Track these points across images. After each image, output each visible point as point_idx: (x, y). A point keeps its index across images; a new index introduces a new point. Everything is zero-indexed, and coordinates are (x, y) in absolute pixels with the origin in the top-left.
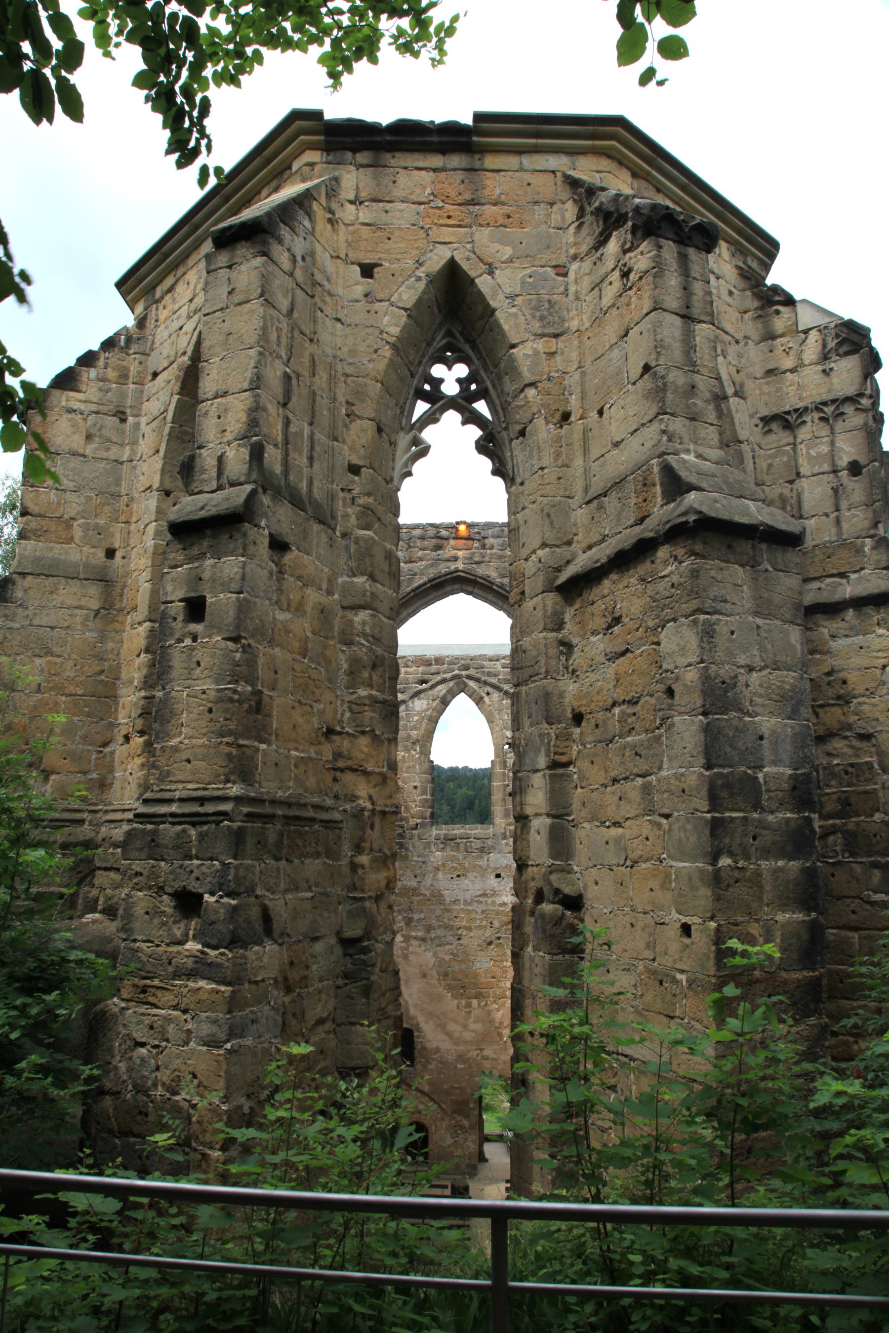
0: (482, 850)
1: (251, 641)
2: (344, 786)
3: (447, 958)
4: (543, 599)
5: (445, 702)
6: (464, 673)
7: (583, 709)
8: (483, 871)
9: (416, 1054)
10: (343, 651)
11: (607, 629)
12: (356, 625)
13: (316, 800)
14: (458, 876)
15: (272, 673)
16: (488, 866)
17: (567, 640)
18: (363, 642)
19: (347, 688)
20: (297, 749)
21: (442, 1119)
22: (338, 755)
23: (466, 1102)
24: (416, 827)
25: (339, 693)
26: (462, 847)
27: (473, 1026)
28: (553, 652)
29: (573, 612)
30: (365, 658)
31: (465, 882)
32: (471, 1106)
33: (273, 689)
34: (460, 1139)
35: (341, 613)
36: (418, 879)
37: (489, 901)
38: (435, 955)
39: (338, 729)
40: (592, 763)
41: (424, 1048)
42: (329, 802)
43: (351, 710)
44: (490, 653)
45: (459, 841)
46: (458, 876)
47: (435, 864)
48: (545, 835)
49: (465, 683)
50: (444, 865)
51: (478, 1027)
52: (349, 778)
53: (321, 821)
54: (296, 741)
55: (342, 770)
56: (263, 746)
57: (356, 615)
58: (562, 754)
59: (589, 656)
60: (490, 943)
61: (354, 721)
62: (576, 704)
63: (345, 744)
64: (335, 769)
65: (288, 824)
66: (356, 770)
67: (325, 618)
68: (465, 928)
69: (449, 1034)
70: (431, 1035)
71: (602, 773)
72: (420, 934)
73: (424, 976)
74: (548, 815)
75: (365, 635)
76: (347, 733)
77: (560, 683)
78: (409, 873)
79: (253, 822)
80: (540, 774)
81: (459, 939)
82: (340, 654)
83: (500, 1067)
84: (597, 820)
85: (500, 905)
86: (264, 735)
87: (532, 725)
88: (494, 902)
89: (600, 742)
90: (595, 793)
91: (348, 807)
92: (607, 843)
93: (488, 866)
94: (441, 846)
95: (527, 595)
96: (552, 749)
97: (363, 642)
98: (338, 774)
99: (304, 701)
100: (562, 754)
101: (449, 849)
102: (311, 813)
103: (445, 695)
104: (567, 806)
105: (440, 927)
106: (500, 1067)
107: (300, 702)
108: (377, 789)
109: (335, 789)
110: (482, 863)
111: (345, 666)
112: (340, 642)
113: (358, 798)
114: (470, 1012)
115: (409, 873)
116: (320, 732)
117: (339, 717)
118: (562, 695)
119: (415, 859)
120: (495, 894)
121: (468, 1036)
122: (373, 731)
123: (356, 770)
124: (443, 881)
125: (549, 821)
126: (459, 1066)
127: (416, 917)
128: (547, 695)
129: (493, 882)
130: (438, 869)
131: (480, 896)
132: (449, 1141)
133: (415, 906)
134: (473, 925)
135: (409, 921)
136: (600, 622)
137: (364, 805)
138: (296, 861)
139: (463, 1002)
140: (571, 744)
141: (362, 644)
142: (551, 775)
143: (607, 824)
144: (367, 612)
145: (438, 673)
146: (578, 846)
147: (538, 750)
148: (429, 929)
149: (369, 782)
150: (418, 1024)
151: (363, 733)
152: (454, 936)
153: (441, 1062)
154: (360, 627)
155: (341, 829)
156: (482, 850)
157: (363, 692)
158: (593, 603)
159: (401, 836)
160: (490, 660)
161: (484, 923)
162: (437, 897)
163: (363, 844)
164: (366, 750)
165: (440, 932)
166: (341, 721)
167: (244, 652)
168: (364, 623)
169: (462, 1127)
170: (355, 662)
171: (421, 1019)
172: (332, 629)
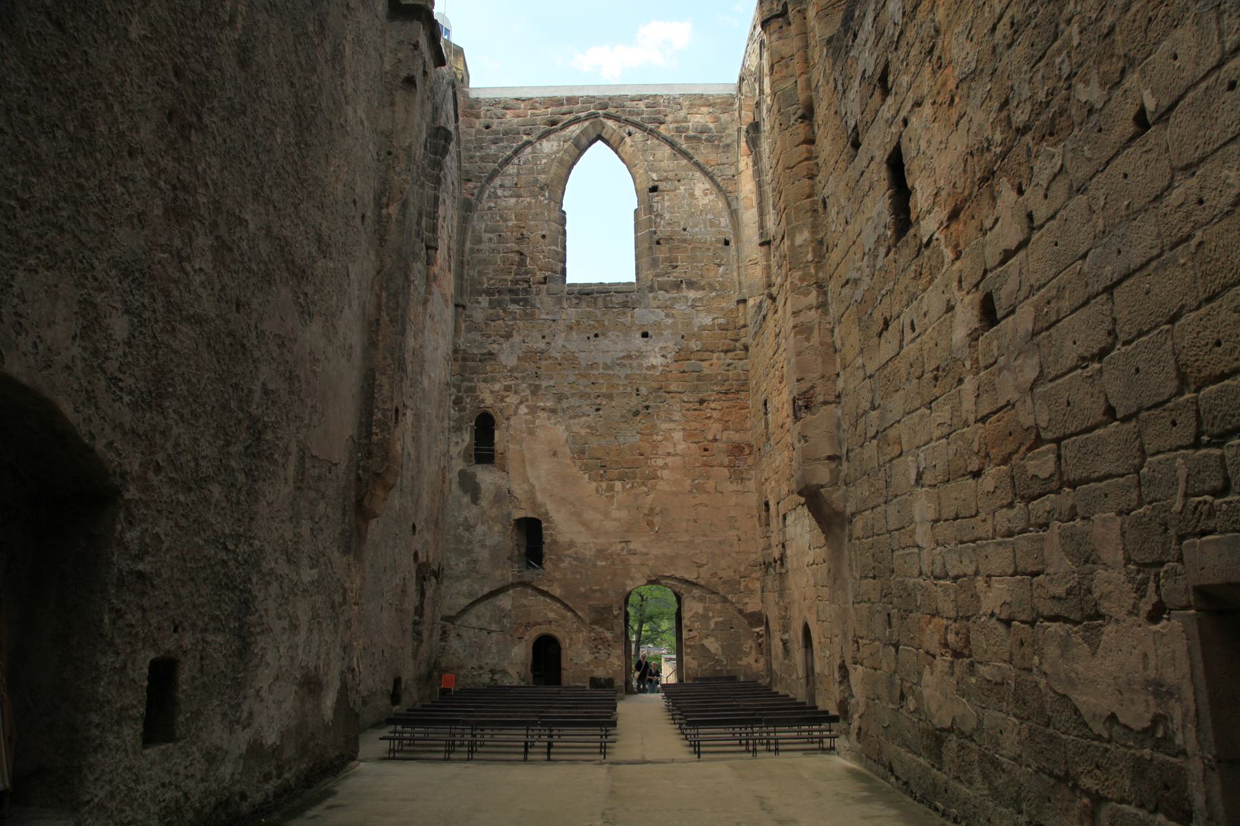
0: (625, 305)
3: (583, 432)
5: (580, 148)
6: (601, 112)
8: (627, 330)
9: (545, 549)
14: (596, 336)
16: (633, 324)
21: (579, 630)
23: (608, 609)
24: (545, 281)
26: (600, 302)
27: (616, 514)
31: (603, 343)
32: (616, 613)
34: (602, 655)
36: (547, 340)
37: (635, 364)
38: (568, 428)
41: (555, 542)
44: (632, 93)
45: (596, 295)
46: (596, 336)
47: (568, 322)
49: (602, 123)
50: (578, 323)
51: (623, 514)
60: (636, 413)
68: (605, 396)
69: (585, 524)
70: (563, 527)
72: (548, 404)
73: (555, 454)
78: (536, 333)
81: (598, 410)
83: (651, 563)
85: (648, 368)
88: (640, 365)
93: (633, 324)
94: (575, 301)
101: (584, 304)
103: (578, 136)
105: (573, 395)
106: (651, 563)
110: (627, 320)
114: (612, 497)
115: (536, 333)
119: (543, 316)
120: (641, 355)
121: (609, 525)
124: (575, 343)
126: (599, 563)
127: (544, 384)
129: (638, 341)
130: (571, 328)
131: (623, 358)
132: (588, 657)
133: (542, 372)
134: (615, 391)
135: (535, 390)
139: (604, 485)
145: (570, 113)
148: (560, 397)
150: (547, 513)
152: (591, 405)
153: (576, 559)
156: (625, 305)
159: (526, 291)
160: (633, 101)
161: (629, 390)
162: (571, 360)
165: (574, 401)
169: (603, 640)
171: (550, 507)
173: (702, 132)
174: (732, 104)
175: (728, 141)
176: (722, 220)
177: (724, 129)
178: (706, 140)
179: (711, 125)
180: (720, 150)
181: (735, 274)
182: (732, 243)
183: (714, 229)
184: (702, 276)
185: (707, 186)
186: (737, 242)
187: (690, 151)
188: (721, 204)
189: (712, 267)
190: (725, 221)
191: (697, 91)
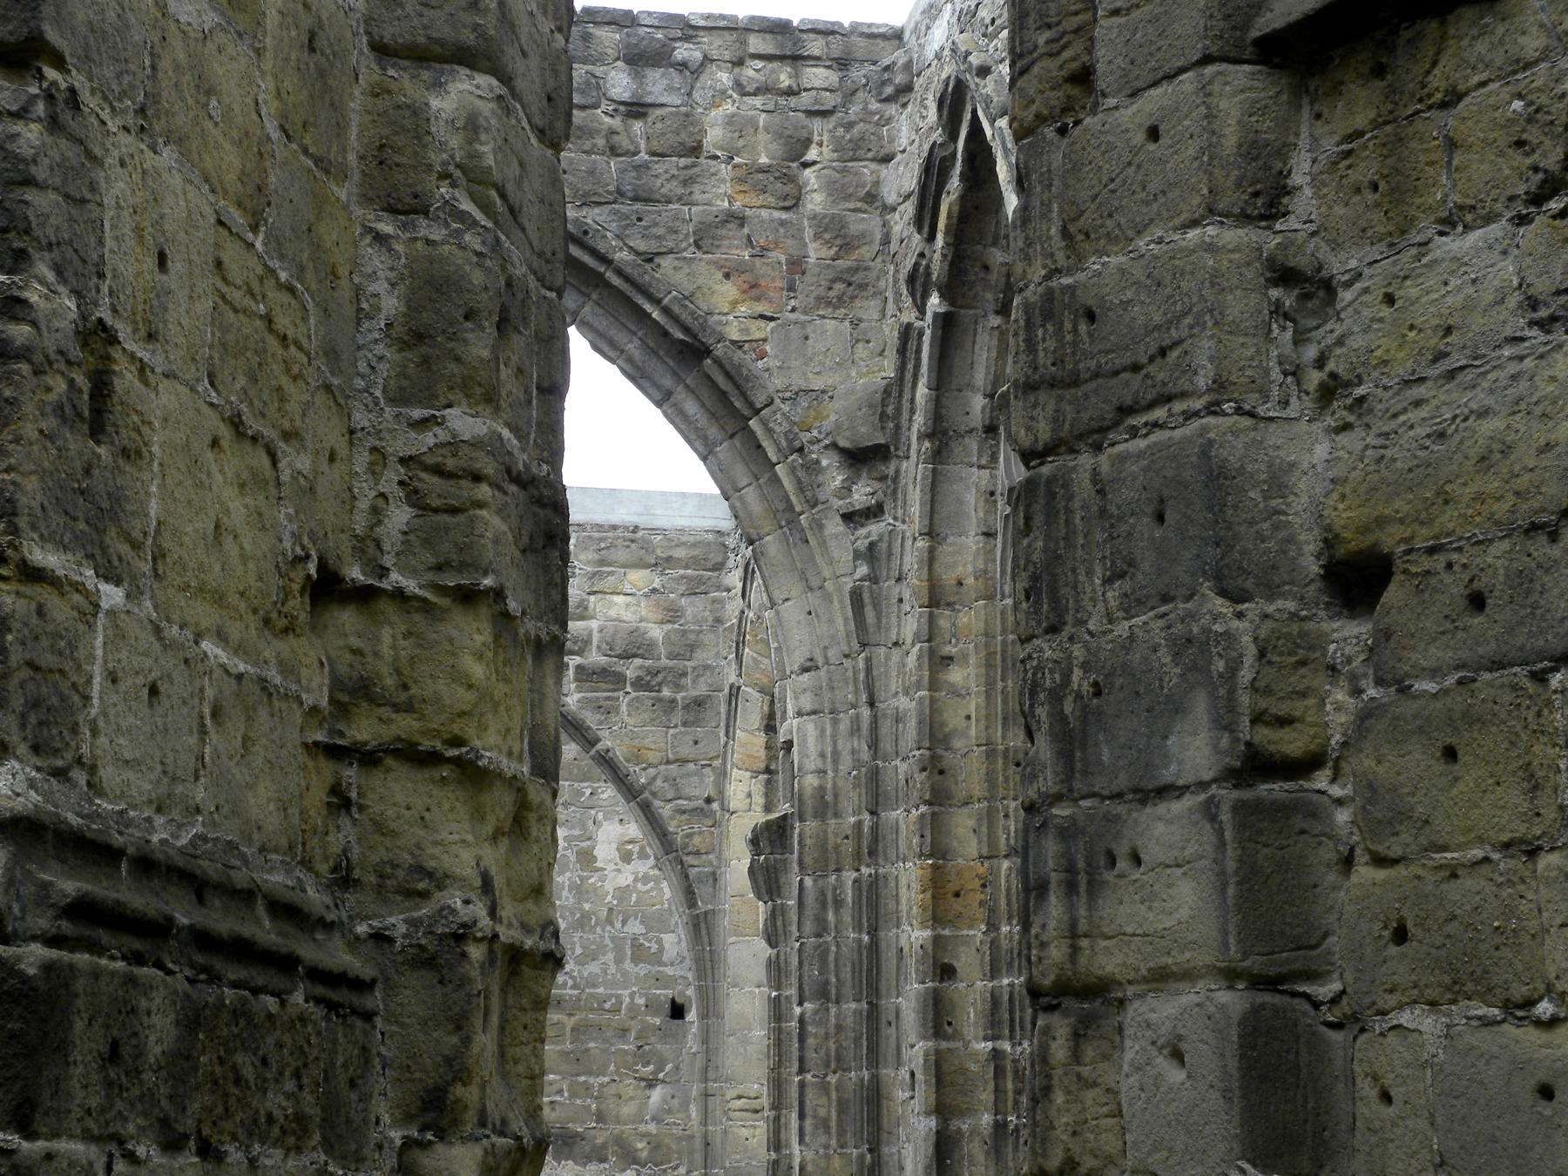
1: (78, 80)
2: (380, 827)
4: (1204, 89)
7: (1390, 539)
10: (380, 239)
11: (1537, 199)
12: (438, 129)
13: (276, 879)
15: (151, 262)
17: (1302, 262)
18: (466, 205)
19: (400, 398)
20: (221, 637)
22: (353, 692)
25: (361, 419)
28: (1243, 304)
29: (1330, 145)
30: (477, 277)
33: (151, 337)
35: (369, 70)
39: (355, 573)
40: (1450, 754)
42: (315, 898)
43: (414, 497)
48: (1212, 1059)
52: (397, 793)
53: (318, 975)
54: (219, 599)
55: (369, 758)
56: (112, 595)
57: (437, 86)
58: (1284, 722)
59: (1427, 315)
61: (427, 543)
62: (1343, 516)
63: (389, 638)
64: (335, 752)
65: (214, 978)
66: (431, 759)
67: (322, 74)
71: (1514, 795)
74: (1230, 976)
75: (474, 177)
76: (399, 595)
77: (1274, 436)
79: (96, 948)
80: (1178, 807)
82: (367, 249)
84: (1485, 996)
86: (112, 539)
87: (1132, 604)
89: (1497, 665)
90: (1468, 882)
91: (396, 923)
92: (1546, 1092)
95: (1105, 76)
96: (1245, 699)
97: (466, 205)
98: (350, 773)
99: (253, 425)
100: (1284, 722)
102: (264, 930)
104: (1309, 941)
107: (236, 423)
108: (504, 844)
109: (336, 842)
111: (391, 304)
112: (366, 199)
113: (441, 880)
116: (298, 576)
117: (360, 524)
118: (1278, 482)
122: (498, 594)
123: (431, 759)
125: (1234, 1001)
128: (1218, 480)
136: (1493, 171)
137: (465, 914)
138: (234, 1155)
140: (1320, 682)
141: (462, 216)
142: (1239, 808)
143: (1545, 1008)
144: (485, 80)
146: (1369, 1108)
147: (1177, 708)
149: (478, 815)
151: (467, 597)
154: (455, 142)
155: (368, 1016)
157: (464, 422)
158: (1453, 98)
163: (459, 1091)
164: (478, 671)
166: (368, 546)
167: (54, 124)
168: (472, 126)
170: (431, 287)
172: (340, 129)
173: (627, 656)
174: (719, 567)
175: (701, 690)
176: (668, 939)
177: (692, 647)
178: (639, 684)
179: (656, 632)
180: (677, 717)
181: (694, 1111)
182: (692, 1015)
183: (642, 969)
184: (600, 1117)
185: (633, 830)
186: (704, 1015)
187: (590, 719)
188: (667, 891)
189: (629, 1087)
190: (674, 943)
191: (623, 515)
